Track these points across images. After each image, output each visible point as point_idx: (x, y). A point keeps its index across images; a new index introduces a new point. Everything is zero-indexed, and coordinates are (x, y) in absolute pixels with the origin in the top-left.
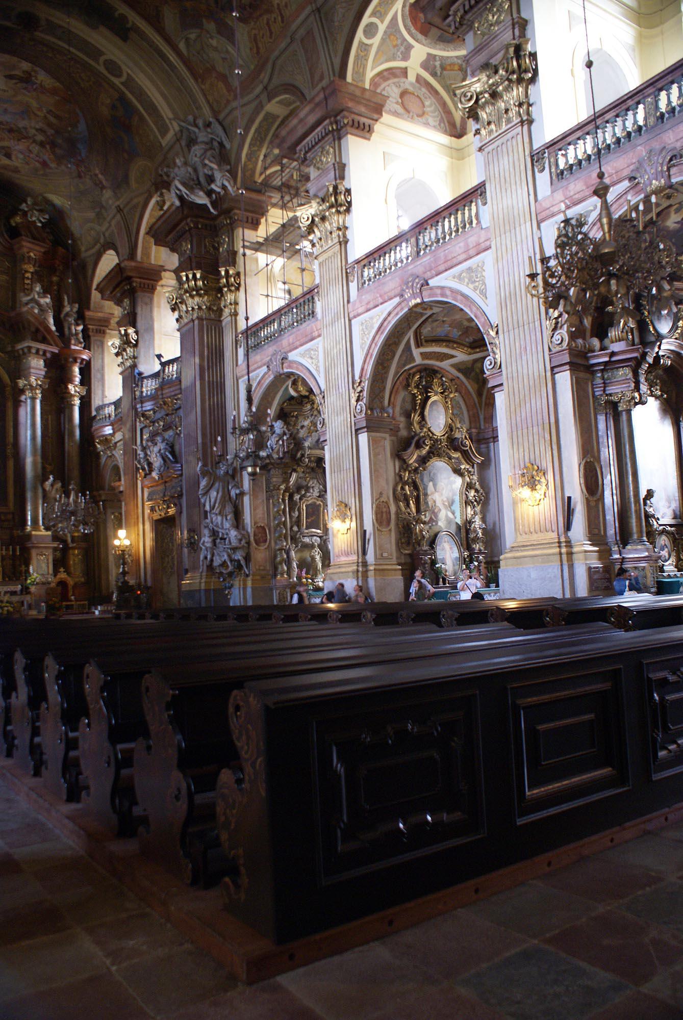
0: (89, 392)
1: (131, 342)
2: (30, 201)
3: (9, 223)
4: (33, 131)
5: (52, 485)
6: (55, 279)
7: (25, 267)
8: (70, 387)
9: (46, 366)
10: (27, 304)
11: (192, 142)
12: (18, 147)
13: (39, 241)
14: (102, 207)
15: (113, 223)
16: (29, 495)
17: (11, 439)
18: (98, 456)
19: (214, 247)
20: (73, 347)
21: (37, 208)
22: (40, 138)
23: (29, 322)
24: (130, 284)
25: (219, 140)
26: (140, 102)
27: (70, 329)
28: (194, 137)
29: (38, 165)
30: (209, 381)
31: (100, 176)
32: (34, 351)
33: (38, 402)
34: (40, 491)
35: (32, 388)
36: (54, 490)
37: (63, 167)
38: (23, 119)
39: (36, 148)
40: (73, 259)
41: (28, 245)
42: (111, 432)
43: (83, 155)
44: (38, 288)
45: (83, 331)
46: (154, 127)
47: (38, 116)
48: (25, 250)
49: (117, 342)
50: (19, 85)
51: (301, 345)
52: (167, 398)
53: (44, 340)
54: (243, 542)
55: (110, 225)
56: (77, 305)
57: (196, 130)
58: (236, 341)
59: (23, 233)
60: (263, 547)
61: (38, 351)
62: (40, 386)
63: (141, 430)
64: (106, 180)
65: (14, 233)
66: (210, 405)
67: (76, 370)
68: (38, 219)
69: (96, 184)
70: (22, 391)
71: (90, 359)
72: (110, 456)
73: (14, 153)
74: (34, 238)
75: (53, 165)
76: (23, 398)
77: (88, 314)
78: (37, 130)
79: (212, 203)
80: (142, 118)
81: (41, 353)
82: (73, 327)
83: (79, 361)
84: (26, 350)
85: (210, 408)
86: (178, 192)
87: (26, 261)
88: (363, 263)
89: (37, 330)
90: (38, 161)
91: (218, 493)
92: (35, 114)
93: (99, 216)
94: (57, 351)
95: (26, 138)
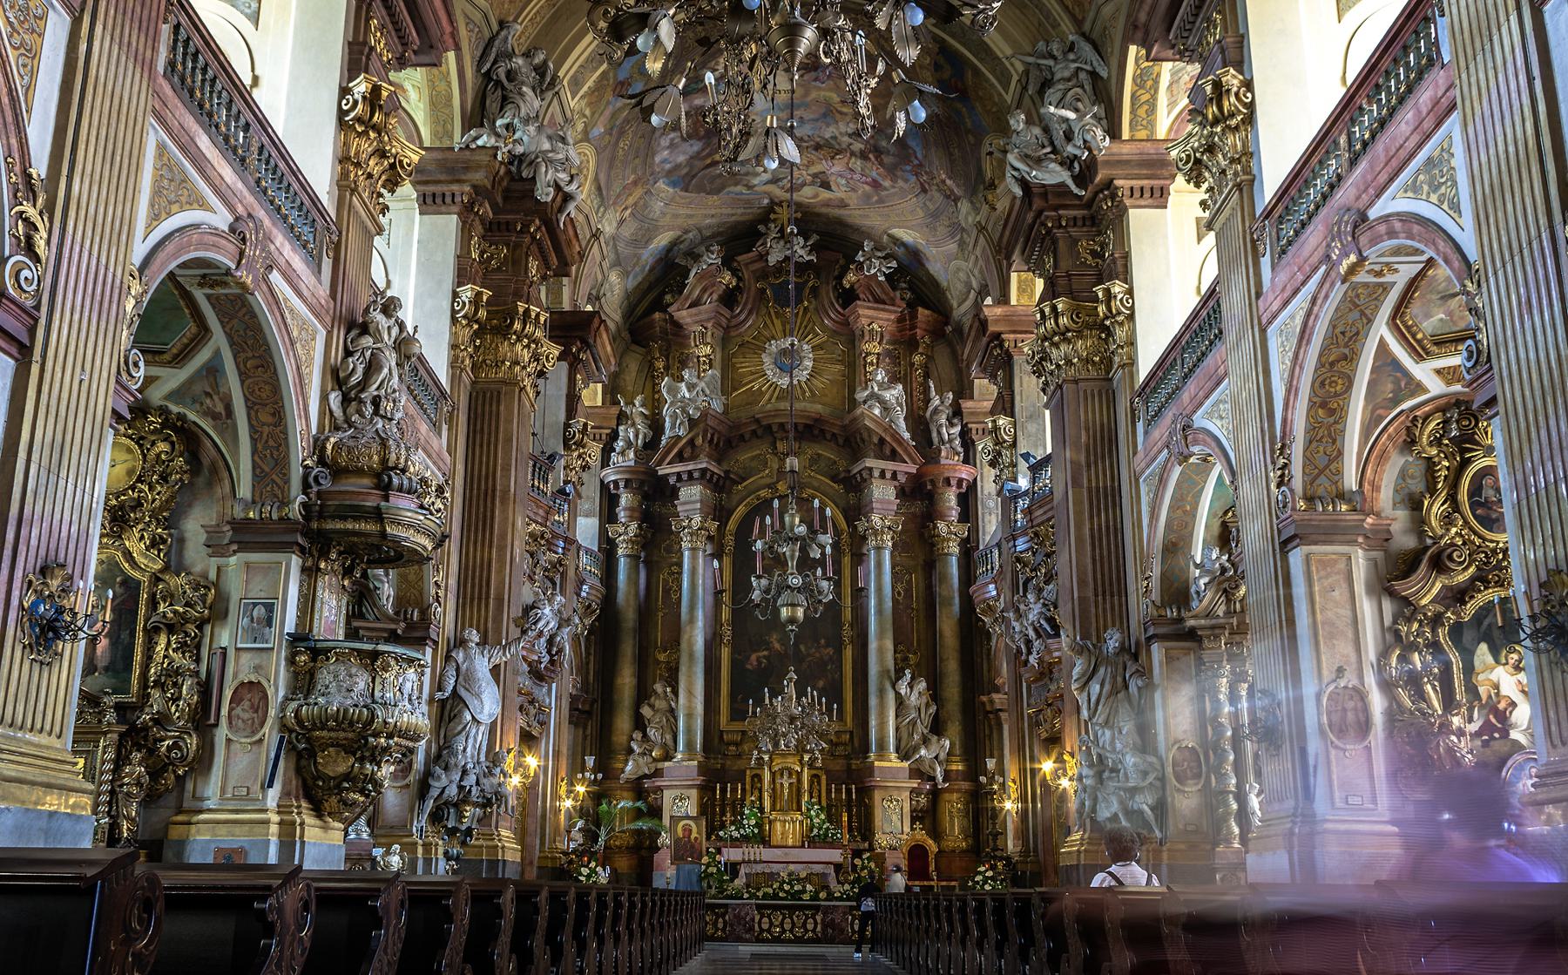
0: (974, 531)
1: (1005, 441)
2: (868, 245)
3: (841, 284)
4: (846, 139)
5: (911, 685)
6: (917, 359)
7: (867, 347)
8: (941, 525)
10: (865, 402)
11: (1046, 84)
12: (835, 168)
13: (884, 303)
14: (963, 230)
16: (873, 701)
17: (847, 615)
18: (988, 636)
19: (1094, 254)
20: (943, 461)
21: (879, 254)
22: (858, 146)
23: (869, 429)
24: (1001, 345)
25: (1088, 68)
26: (964, 45)
27: (939, 433)
28: (1049, 77)
29: (867, 188)
30: (1090, 490)
31: (948, 182)
32: (876, 474)
33: (887, 555)
34: (891, 696)
35: (876, 533)
36: (915, 692)
37: (901, 183)
38: (828, 125)
39: (857, 164)
40: (947, 324)
41: (867, 312)
42: (994, 593)
43: (919, 156)
46: (991, 77)
47: (846, 114)
48: (864, 321)
49: (990, 446)
50: (806, 77)
51: (1207, 397)
52: (1039, 525)
53: (894, 456)
54: (1151, 778)
56: (951, 395)
57: (1051, 62)
58: (1133, 411)
59: (861, 296)
60: (1192, 787)
61: (882, 475)
62: (889, 528)
64: (958, 186)
65: (848, 297)
66: (1092, 529)
67: (951, 498)
68: (878, 269)
69: (948, 197)
70: (864, 538)
71: (975, 479)
73: (832, 178)
74: (878, 300)
75: (887, 183)
77: (967, 405)
78: (850, 136)
79: (1075, 178)
80: (976, 72)
81: (888, 475)
83: (953, 482)
85: (1092, 537)
86: (1016, 174)
87: (867, 338)
88: (1276, 214)
89: (882, 441)
90: (866, 183)
91: (1102, 686)
92: (841, 113)
93: (962, 244)
95: (839, 152)
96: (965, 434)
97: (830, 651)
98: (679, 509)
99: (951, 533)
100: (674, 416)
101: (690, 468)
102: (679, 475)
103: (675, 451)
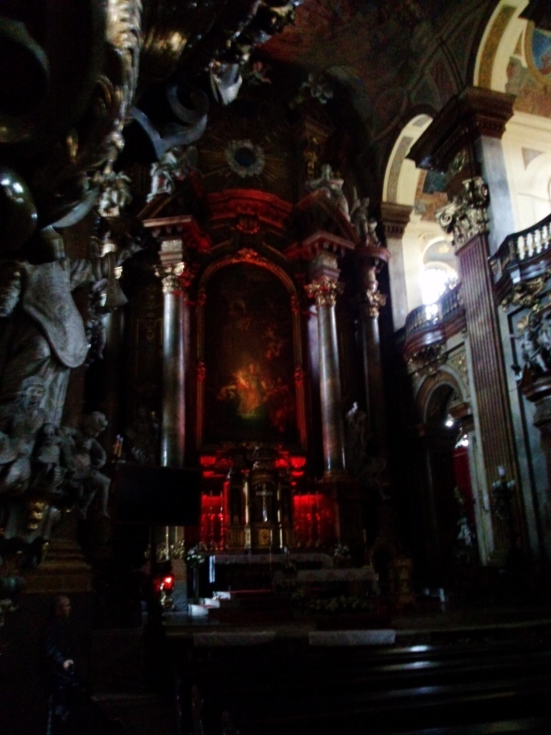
8: (369, 294)
9: (339, 267)
15: (427, 72)
29: (326, 22)
33: (333, 310)
37: (359, 15)
44: (328, 170)
45: (377, 229)
48: (307, 134)
55: (423, 75)
63: (510, 317)
72: (434, 376)
75: (345, 18)
76: (313, 309)
81: (335, 249)
82: (366, 225)
83: (377, 263)
84: (317, 245)
94: (353, 247)
96: (380, 231)
97: (286, 387)
98: (163, 258)
99: (374, 300)
100: (162, 177)
101: (175, 222)
102: (162, 228)
103: (160, 208)
